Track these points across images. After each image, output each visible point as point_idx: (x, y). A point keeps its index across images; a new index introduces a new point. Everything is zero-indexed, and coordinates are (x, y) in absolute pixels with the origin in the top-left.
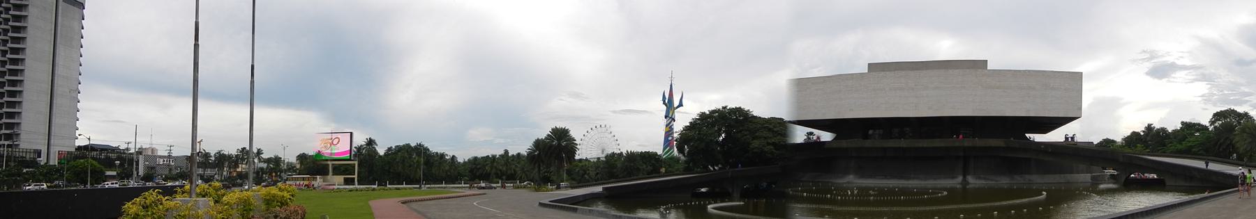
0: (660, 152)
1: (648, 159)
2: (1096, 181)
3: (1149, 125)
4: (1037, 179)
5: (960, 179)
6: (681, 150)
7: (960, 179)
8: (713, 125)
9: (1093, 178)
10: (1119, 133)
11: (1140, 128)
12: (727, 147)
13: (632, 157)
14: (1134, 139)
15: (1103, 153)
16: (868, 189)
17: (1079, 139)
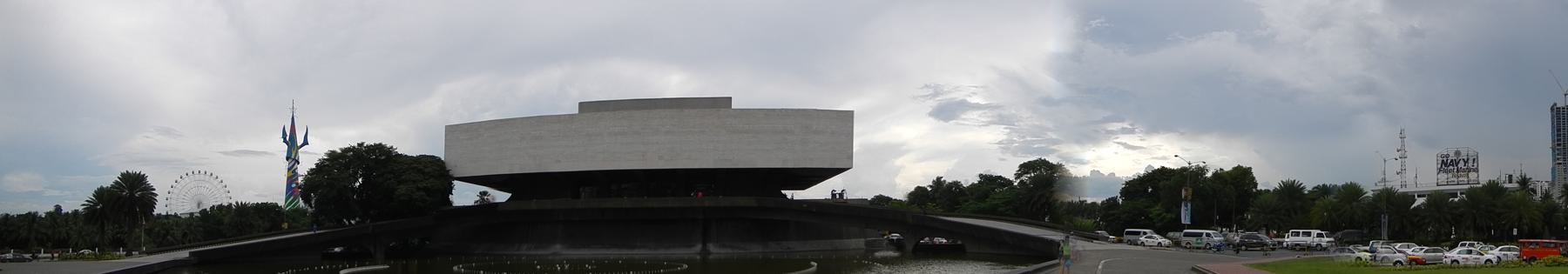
0: (281, 203)
1: (265, 213)
2: (872, 247)
3: (939, 179)
4: (798, 247)
5: (699, 247)
6: (307, 201)
7: (699, 247)
8: (347, 166)
9: (867, 244)
10: (900, 187)
11: (927, 183)
12: (369, 198)
13: (243, 209)
14: (919, 195)
15: (879, 212)
16: (583, 262)
17: (848, 196)
